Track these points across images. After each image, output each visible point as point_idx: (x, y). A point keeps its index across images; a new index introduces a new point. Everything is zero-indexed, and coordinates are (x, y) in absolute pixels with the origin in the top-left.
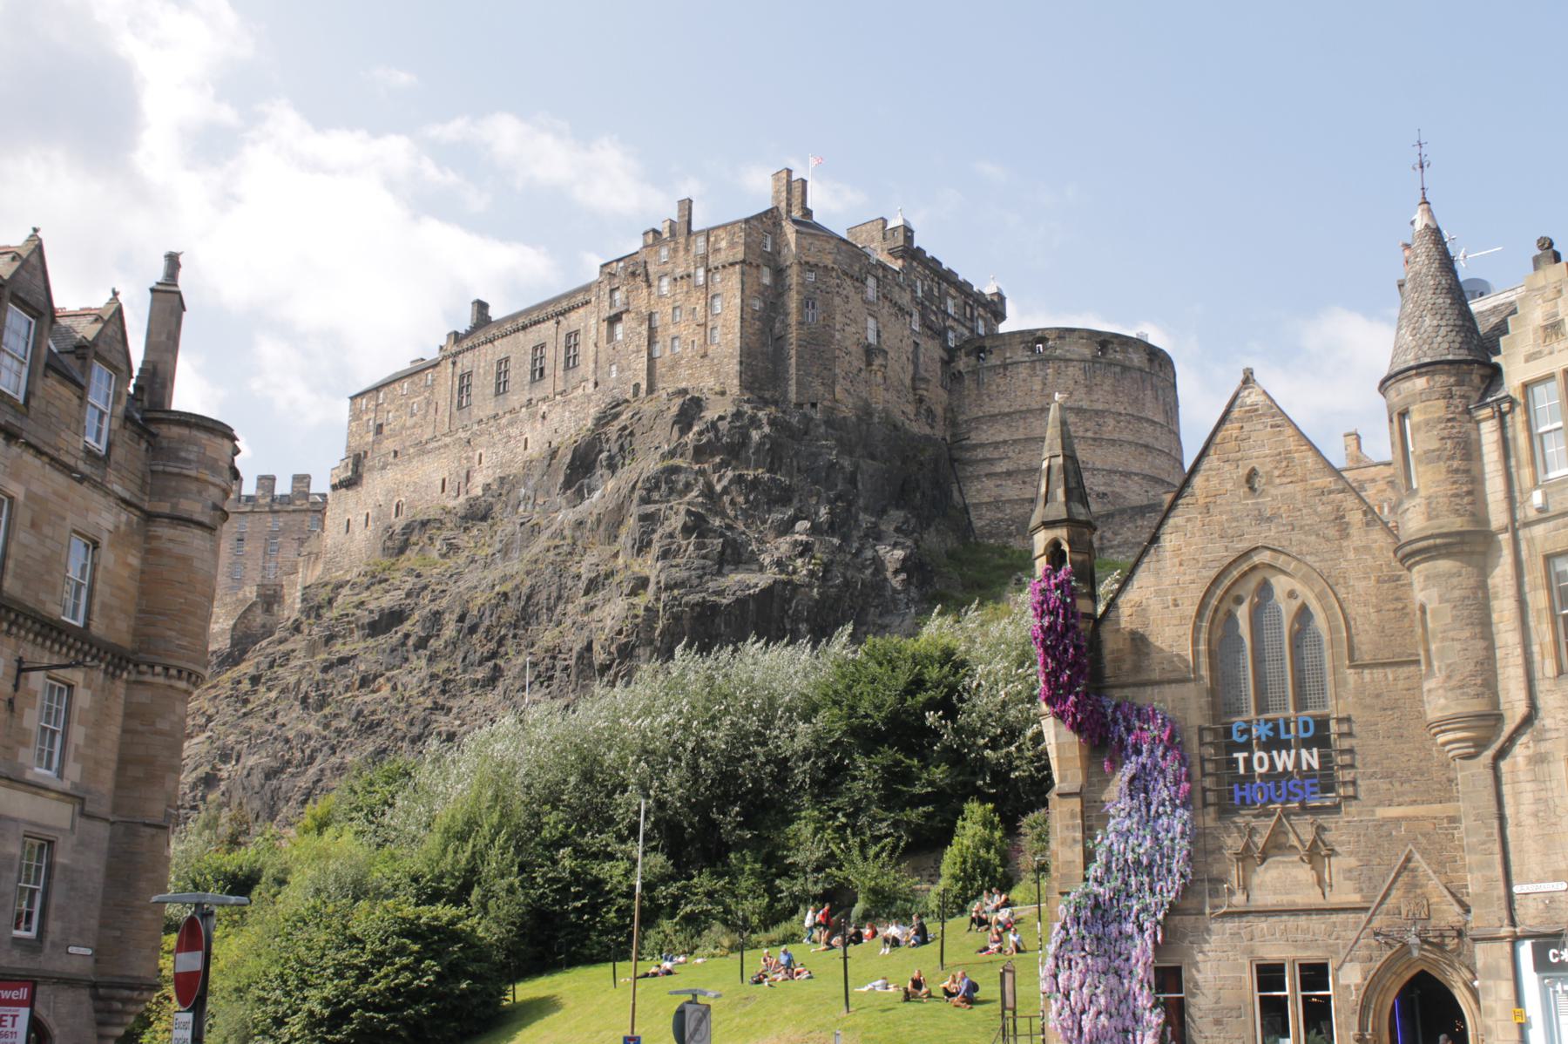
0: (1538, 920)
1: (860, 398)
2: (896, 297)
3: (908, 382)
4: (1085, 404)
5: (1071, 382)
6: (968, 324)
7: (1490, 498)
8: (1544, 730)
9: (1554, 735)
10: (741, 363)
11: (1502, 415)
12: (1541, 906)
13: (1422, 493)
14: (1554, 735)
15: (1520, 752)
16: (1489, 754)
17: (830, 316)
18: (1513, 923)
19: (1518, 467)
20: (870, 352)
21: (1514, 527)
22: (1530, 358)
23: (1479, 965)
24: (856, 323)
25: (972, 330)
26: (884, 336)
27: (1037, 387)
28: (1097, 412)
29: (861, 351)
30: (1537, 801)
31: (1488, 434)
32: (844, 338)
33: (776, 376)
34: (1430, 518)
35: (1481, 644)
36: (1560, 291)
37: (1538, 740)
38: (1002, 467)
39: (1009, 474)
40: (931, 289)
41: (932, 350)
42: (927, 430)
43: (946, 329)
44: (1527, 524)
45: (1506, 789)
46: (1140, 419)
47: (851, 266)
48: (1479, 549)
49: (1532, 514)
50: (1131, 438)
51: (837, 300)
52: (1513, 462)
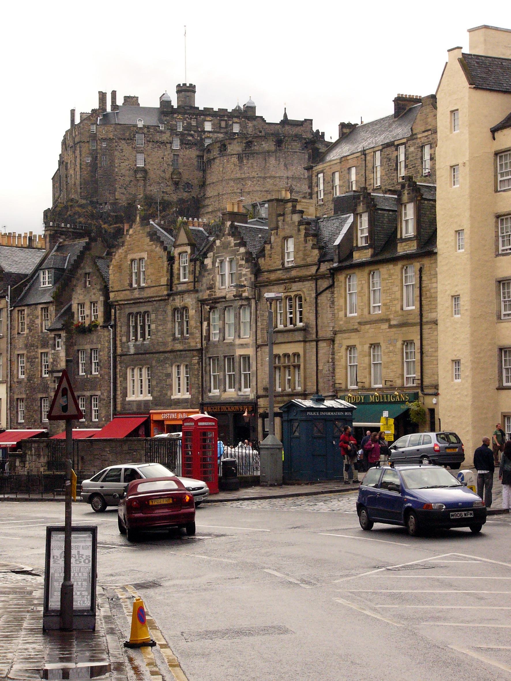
1: (130, 194)
2: (158, 137)
3: (168, 175)
4: (238, 176)
5: (233, 166)
6: (222, 131)
10: (81, 188)
17: (113, 161)
20: (137, 170)
24: (128, 159)
25: (226, 133)
26: (149, 159)
27: (221, 169)
28: (242, 179)
29: (132, 172)
32: (120, 170)
33: (96, 190)
38: (210, 209)
39: (212, 212)
40: (189, 124)
41: (193, 153)
42: (185, 195)
43: (202, 140)
46: (265, 178)
47: (124, 134)
50: (258, 189)
51: (116, 153)
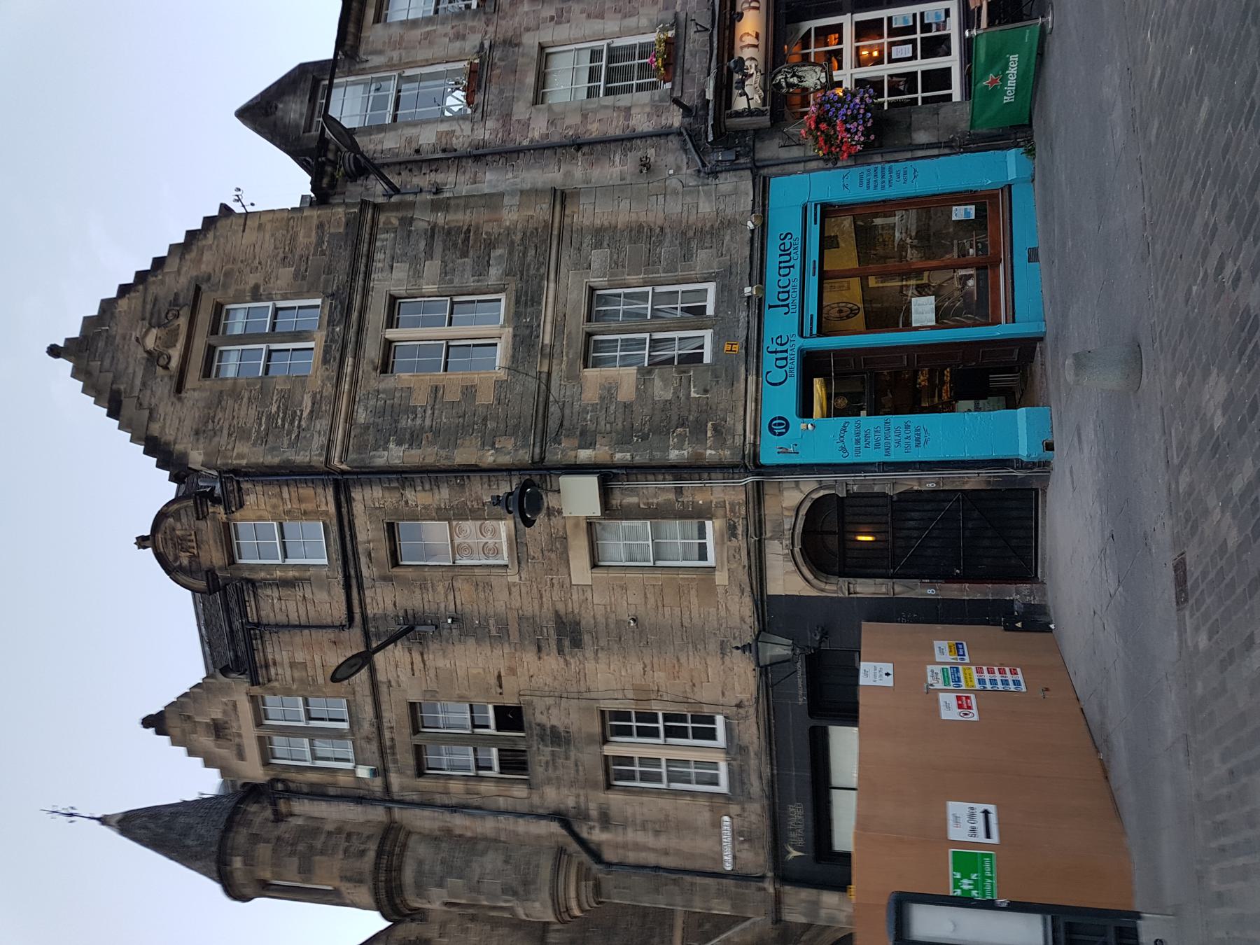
0: (760, 851)
7: (362, 819)
8: (577, 808)
9: (582, 799)
11: (287, 790)
12: (746, 846)
13: (337, 883)
14: (582, 799)
15: (597, 836)
16: (596, 867)
18: (762, 878)
19: (334, 785)
21: (388, 798)
22: (241, 756)
23: (803, 920)
30: (644, 829)
31: (303, 807)
34: (361, 881)
35: (491, 856)
36: (189, 717)
37: (586, 817)
44: (387, 787)
45: (632, 857)
48: (402, 836)
49: (378, 782)
52: (332, 791)
